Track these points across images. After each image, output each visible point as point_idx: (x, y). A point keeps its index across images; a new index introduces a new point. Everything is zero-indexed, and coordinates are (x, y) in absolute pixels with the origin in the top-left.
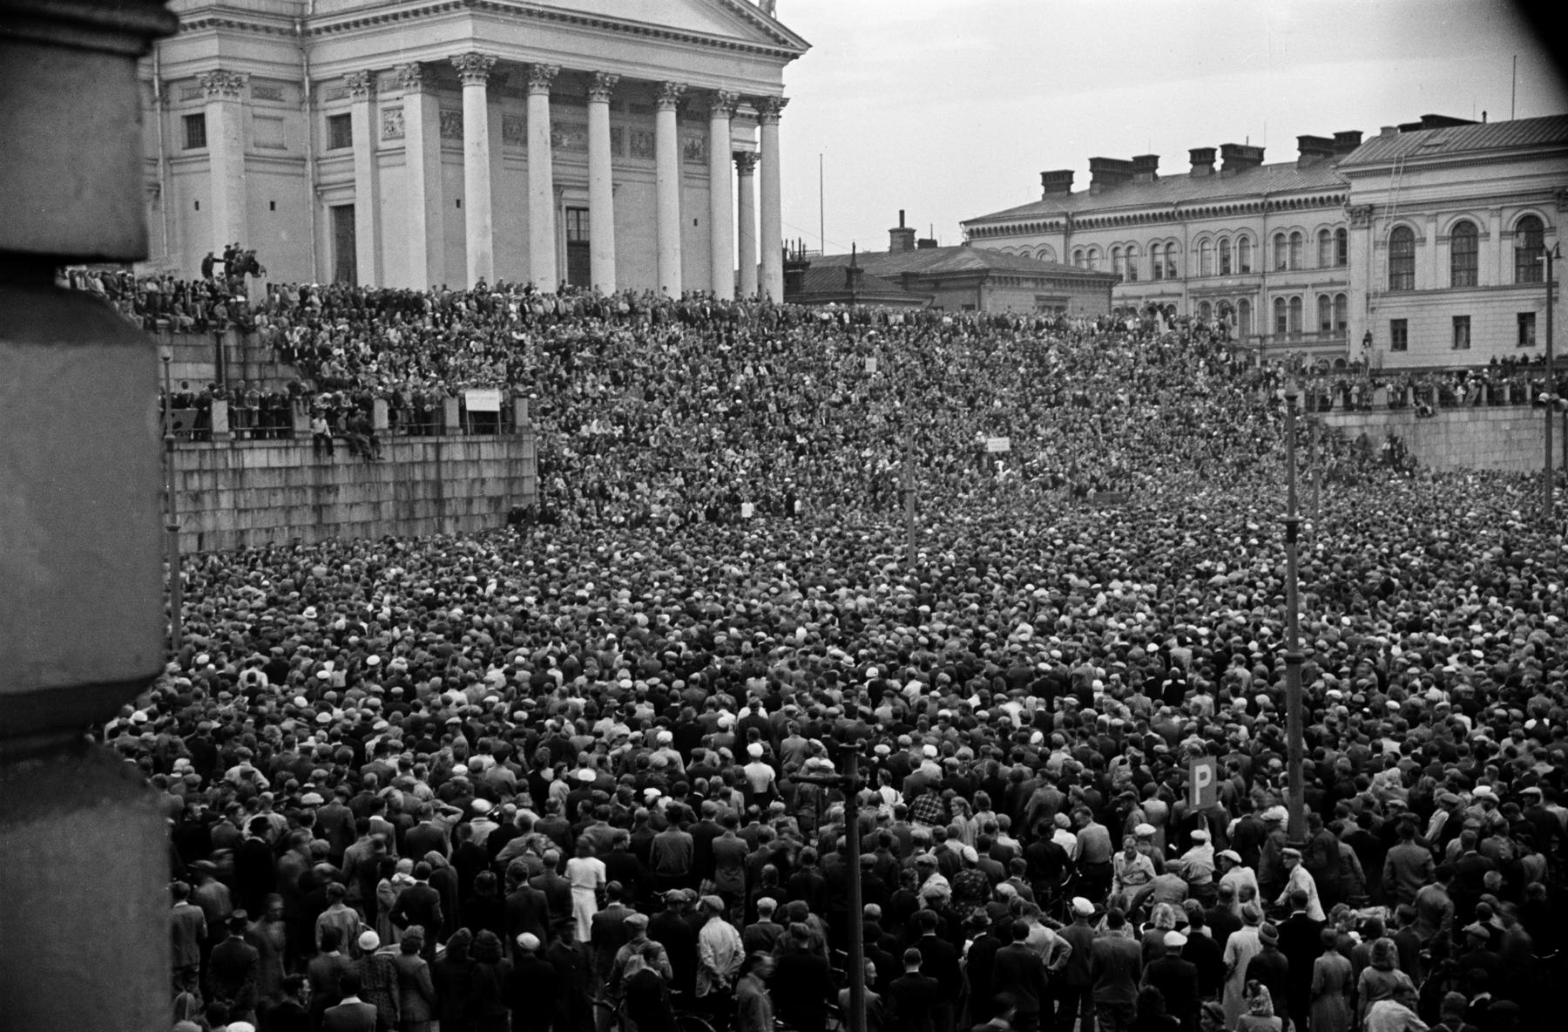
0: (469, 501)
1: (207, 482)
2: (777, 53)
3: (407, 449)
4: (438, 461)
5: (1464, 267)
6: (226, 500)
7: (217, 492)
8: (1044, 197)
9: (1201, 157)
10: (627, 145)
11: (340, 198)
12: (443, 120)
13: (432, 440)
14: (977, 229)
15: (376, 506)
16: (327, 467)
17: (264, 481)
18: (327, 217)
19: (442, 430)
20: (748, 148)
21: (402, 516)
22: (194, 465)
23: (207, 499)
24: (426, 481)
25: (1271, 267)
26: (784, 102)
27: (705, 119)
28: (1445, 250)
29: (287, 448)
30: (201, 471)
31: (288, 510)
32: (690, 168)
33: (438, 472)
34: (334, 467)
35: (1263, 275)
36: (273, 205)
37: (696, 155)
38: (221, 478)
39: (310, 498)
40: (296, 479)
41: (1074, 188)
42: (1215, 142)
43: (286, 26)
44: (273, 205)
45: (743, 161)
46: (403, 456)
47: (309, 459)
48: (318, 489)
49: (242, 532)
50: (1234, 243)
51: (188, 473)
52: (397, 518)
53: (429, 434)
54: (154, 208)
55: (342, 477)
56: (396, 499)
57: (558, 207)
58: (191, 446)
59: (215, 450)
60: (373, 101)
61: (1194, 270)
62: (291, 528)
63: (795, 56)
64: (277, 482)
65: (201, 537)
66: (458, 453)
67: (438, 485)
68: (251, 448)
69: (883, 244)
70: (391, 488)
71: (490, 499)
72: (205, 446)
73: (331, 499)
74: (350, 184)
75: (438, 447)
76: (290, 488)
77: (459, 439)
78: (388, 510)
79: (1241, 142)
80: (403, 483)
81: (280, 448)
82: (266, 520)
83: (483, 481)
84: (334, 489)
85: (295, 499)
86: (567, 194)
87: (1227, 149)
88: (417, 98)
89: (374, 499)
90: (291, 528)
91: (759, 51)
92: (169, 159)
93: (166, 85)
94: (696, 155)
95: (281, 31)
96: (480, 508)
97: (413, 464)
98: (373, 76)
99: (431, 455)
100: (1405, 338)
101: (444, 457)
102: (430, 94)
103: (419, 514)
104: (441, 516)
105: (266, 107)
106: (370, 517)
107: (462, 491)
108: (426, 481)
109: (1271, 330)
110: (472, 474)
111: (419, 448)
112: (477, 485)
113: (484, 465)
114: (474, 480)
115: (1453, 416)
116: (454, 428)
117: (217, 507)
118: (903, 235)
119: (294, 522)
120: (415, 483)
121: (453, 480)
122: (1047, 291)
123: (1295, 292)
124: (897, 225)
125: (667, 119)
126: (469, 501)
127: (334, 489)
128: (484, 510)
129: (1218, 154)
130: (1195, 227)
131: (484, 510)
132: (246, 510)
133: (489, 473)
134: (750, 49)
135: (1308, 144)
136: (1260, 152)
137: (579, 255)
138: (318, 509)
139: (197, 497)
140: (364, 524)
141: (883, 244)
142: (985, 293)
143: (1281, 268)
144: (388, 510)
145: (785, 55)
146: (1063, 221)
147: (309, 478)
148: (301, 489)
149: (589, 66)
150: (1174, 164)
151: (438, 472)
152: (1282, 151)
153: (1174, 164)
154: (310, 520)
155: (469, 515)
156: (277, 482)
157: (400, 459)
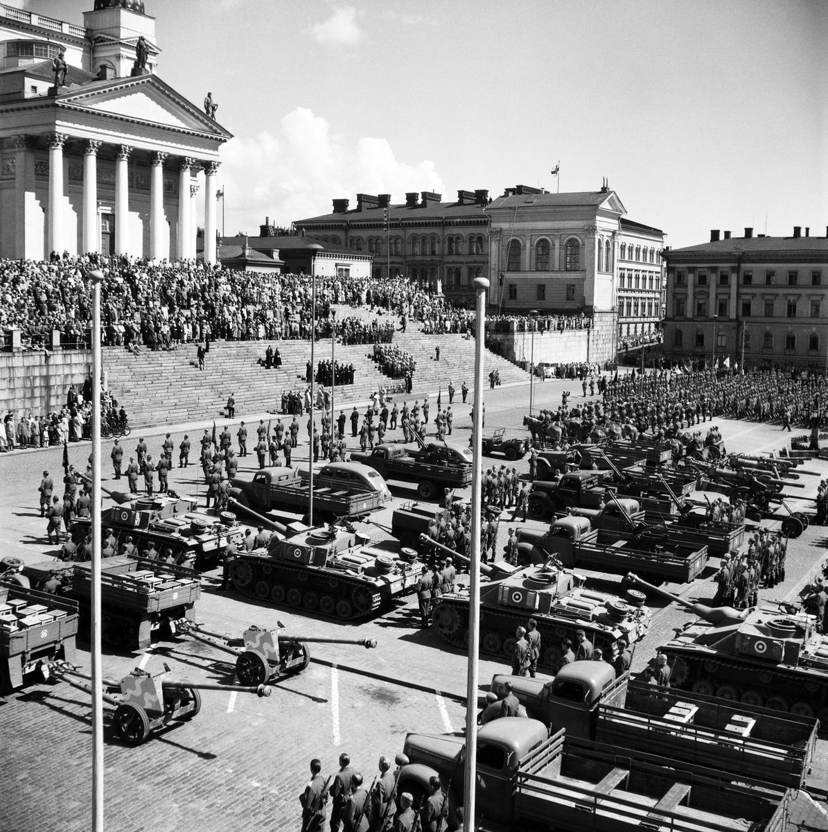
3: (30, 358)
8: (334, 211)
9: (411, 197)
12: (36, 165)
14: (300, 225)
21: (29, 395)
25: (446, 252)
41: (350, 208)
42: (419, 190)
46: (29, 361)
61: (410, 252)
63: (225, 141)
67: (47, 378)
77: (59, 352)
78: (19, 394)
83: (72, 375)
87: (424, 195)
88: (22, 154)
94: (172, 192)
97: (34, 366)
100: (515, 293)
101: (51, 362)
102: (33, 152)
103: (37, 393)
104: (49, 396)
110: (67, 371)
112: (69, 377)
113: (74, 366)
114: (67, 375)
116: (57, 347)
120: (35, 377)
123: (458, 265)
124: (265, 224)
125: (158, 171)
129: (420, 196)
130: (410, 231)
133: (75, 370)
143: (451, 253)
145: (220, 140)
146: (345, 224)
153: (398, 199)
157: (26, 364)
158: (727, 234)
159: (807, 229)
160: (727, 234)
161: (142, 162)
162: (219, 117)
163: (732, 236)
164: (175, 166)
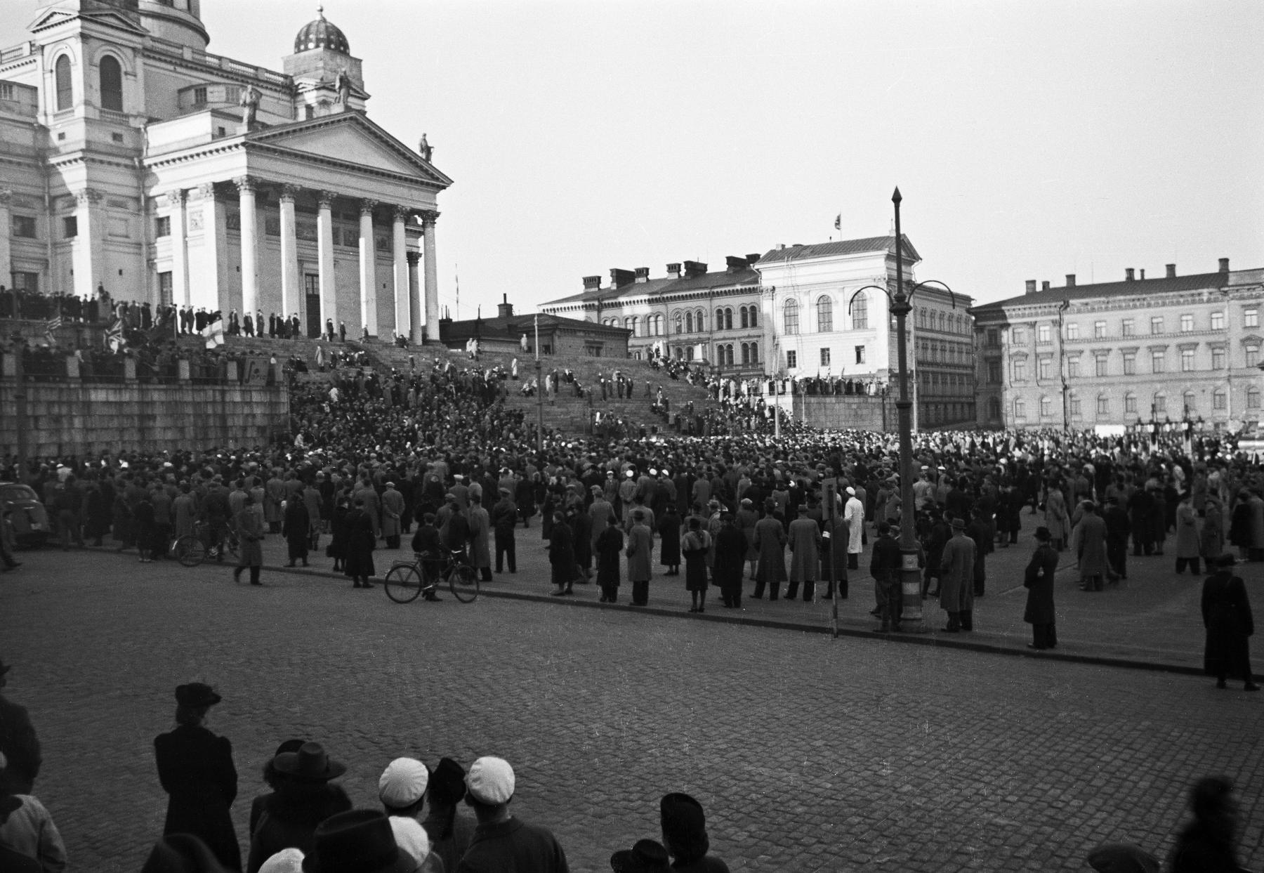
0: (245, 429)
1: (64, 410)
2: (433, 185)
4: (223, 402)
5: (825, 323)
6: (77, 422)
7: (71, 417)
9: (673, 268)
10: (342, 237)
11: (161, 268)
12: (228, 218)
13: (219, 388)
15: (182, 430)
16: (147, 403)
17: (105, 410)
18: (155, 279)
19: (225, 381)
20: (415, 250)
21: (200, 437)
22: (54, 397)
23: (65, 421)
24: (215, 415)
25: (715, 328)
26: (438, 215)
27: (389, 225)
28: (814, 311)
29: (120, 389)
30: (60, 403)
31: (122, 430)
32: (381, 253)
33: (224, 409)
34: (153, 403)
35: (711, 332)
36: (120, 272)
37: (384, 246)
38: (74, 407)
39: (136, 423)
40: (127, 410)
43: (128, 162)
44: (120, 272)
45: (412, 258)
46: (200, 397)
47: (136, 396)
48: (144, 417)
49: (90, 444)
50: (694, 315)
51: (50, 404)
52: (196, 438)
53: (216, 384)
54: (45, 274)
55: (158, 410)
56: (195, 425)
57: (301, 273)
58: (53, 385)
59: (69, 389)
60: (184, 207)
62: (124, 442)
63: (444, 188)
64: (113, 411)
65: (60, 446)
66: (238, 398)
67: (223, 417)
68: (95, 388)
69: (494, 313)
70: (192, 419)
71: (259, 427)
72: (64, 386)
73: (151, 424)
74: (170, 259)
75: (223, 393)
76: (124, 416)
78: (190, 433)
79: (695, 260)
80: (200, 415)
81: (115, 389)
82: (106, 437)
83: (254, 416)
84: (153, 417)
85: (126, 423)
86: (306, 265)
87: (687, 263)
89: (179, 424)
90: (124, 442)
91: (422, 183)
92: (55, 245)
93: (53, 199)
95: (126, 166)
96: (251, 433)
97: (206, 403)
98: (184, 194)
99: (218, 398)
101: (227, 399)
105: (117, 213)
106: (178, 436)
107: (239, 422)
108: (215, 415)
109: (716, 364)
110: (247, 410)
111: (210, 394)
114: (247, 415)
115: (828, 400)
117: (71, 426)
118: (506, 308)
119: (126, 438)
120: (208, 416)
121: (234, 414)
122: (593, 338)
123: (729, 342)
125: (366, 222)
126: (245, 429)
127: (153, 417)
128: (255, 434)
129: (683, 267)
131: (255, 434)
132: (92, 430)
133: (258, 411)
134: (417, 182)
135: (731, 261)
136: (705, 266)
137: (312, 302)
138: (142, 430)
139: (57, 419)
140: (174, 442)
141: (494, 313)
142: (556, 338)
144: (190, 433)
146: (596, 303)
147: (136, 410)
148: (130, 416)
149: (318, 187)
150: (658, 272)
151: (224, 409)
152: (717, 265)
154: (136, 437)
155: (245, 437)
156: (113, 411)
157: (198, 399)
158: (1046, 284)
159: (1142, 271)
160: (1046, 284)
161: (348, 210)
162: (437, 161)
163: (1051, 286)
164: (385, 215)
